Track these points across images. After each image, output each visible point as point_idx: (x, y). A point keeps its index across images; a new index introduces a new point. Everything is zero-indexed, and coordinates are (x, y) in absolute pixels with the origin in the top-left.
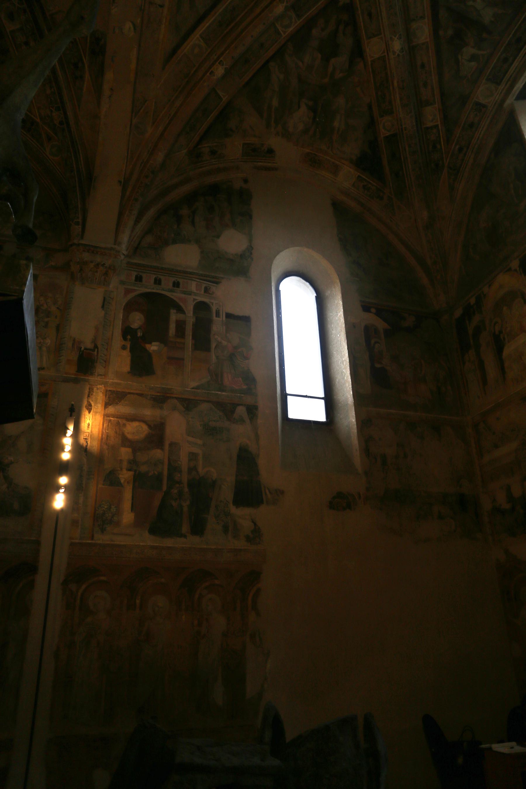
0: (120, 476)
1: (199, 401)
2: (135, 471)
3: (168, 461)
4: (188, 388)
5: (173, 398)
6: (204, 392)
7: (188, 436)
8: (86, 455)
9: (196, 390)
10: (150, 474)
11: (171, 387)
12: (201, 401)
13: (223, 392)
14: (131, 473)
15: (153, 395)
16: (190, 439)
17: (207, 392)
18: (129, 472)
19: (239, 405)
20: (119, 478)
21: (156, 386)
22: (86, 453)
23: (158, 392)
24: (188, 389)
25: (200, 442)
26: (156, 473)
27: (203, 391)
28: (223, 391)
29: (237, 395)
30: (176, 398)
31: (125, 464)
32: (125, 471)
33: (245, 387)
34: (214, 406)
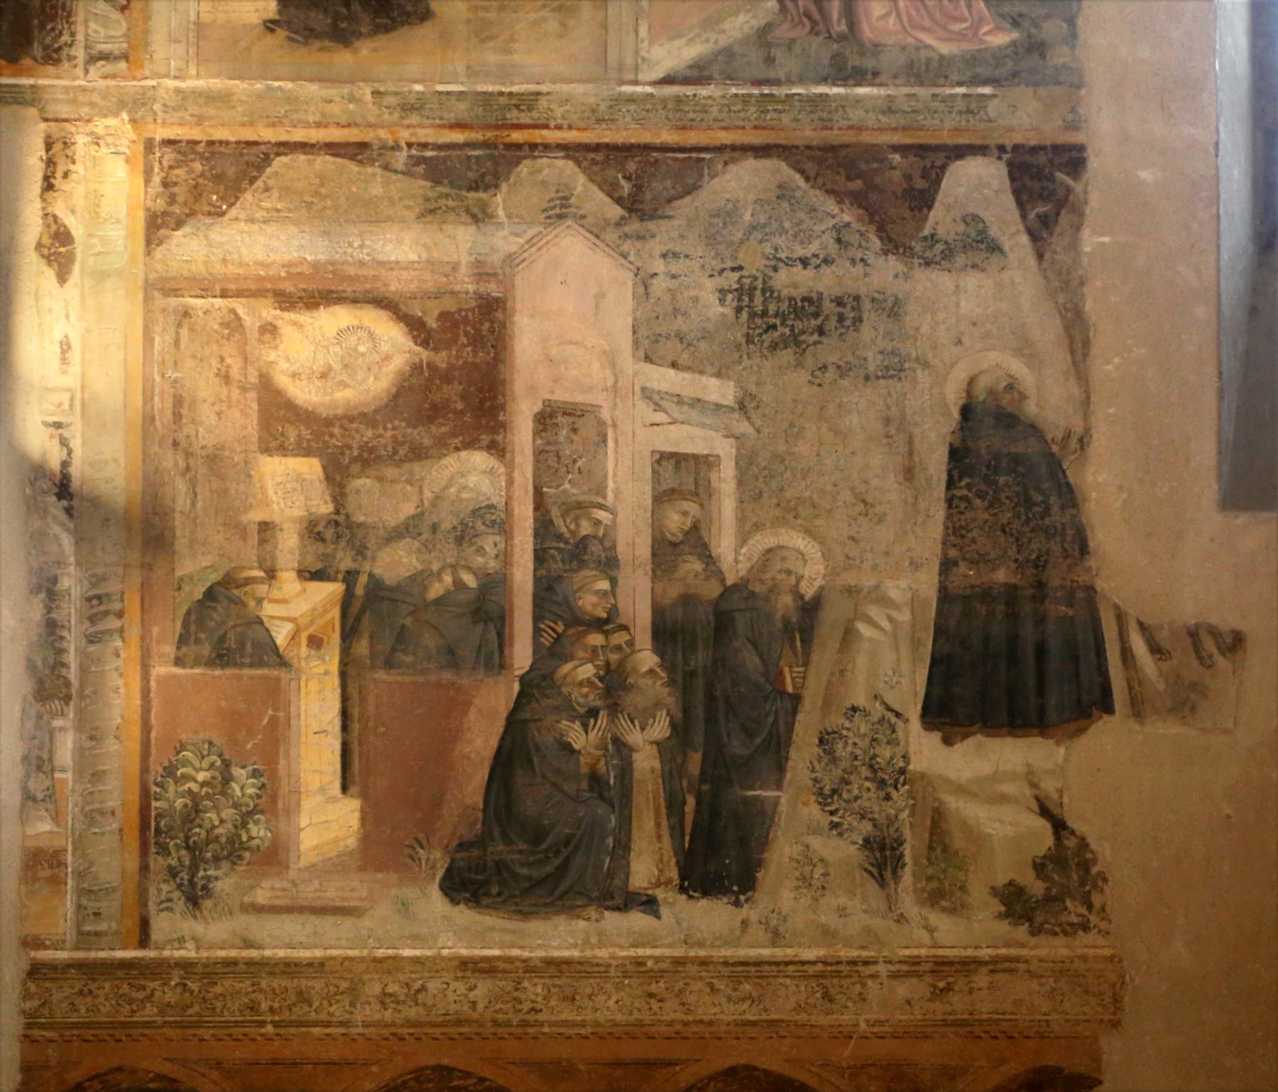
0: (269, 610)
1: (707, 156)
2: (350, 577)
3: (536, 509)
4: (636, 83)
5: (546, 147)
6: (736, 95)
7: (647, 359)
8: (69, 511)
9: (689, 90)
10: (436, 590)
11: (532, 87)
12: (720, 149)
13: (858, 84)
14: (331, 590)
15: (425, 146)
16: (663, 378)
17: (756, 91)
18: (314, 586)
19: (961, 152)
20: (262, 623)
21: (440, 88)
22: (65, 503)
23: (459, 126)
24: (639, 89)
25: (719, 391)
26: (470, 580)
27: (734, 90)
28: (859, 76)
29: (948, 91)
30: (568, 149)
31: (289, 544)
32: (289, 582)
33: (1000, 39)
34: (802, 172)
